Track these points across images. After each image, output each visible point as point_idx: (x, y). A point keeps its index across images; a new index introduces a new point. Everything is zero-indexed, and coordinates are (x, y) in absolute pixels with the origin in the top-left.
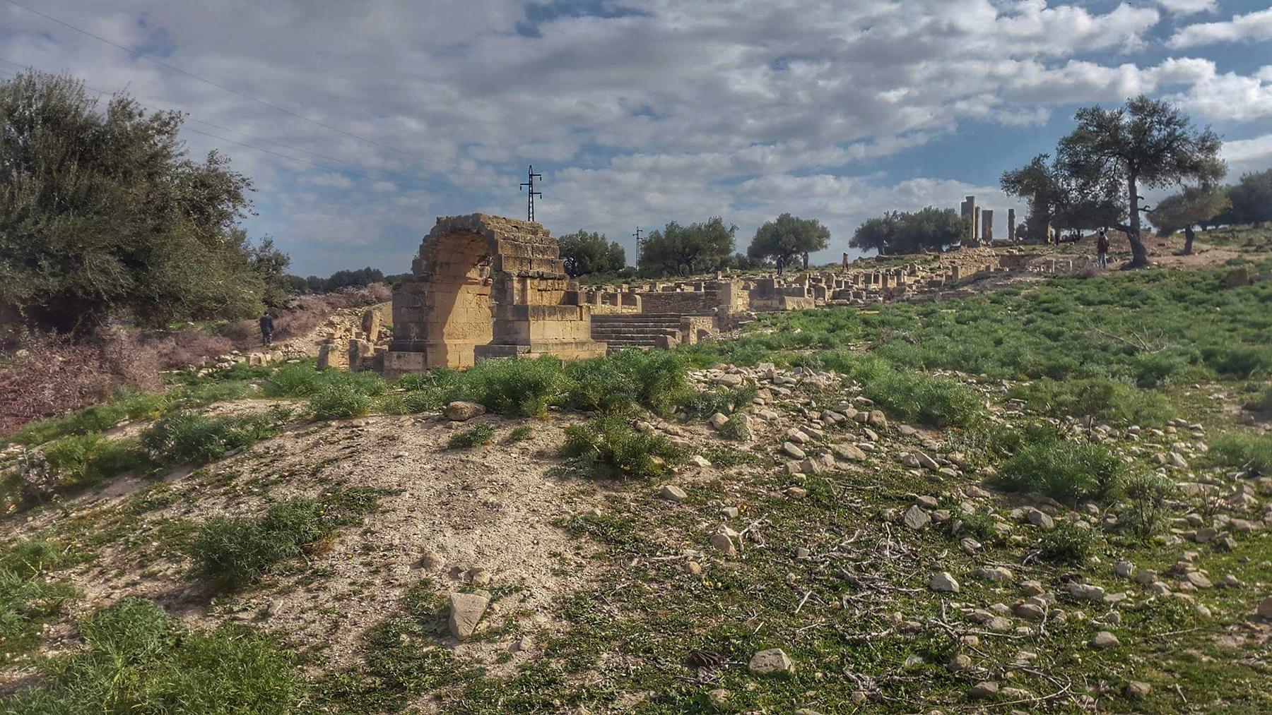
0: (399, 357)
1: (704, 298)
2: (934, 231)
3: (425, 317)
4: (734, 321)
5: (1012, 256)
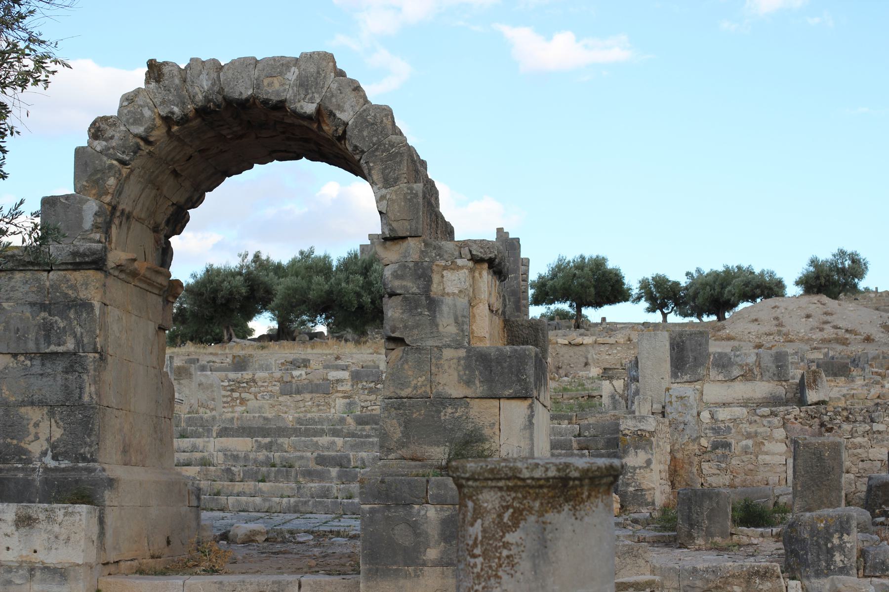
0: (24, 522)
1: (347, 387)
2: (358, 295)
3: (90, 390)
4: (716, 431)
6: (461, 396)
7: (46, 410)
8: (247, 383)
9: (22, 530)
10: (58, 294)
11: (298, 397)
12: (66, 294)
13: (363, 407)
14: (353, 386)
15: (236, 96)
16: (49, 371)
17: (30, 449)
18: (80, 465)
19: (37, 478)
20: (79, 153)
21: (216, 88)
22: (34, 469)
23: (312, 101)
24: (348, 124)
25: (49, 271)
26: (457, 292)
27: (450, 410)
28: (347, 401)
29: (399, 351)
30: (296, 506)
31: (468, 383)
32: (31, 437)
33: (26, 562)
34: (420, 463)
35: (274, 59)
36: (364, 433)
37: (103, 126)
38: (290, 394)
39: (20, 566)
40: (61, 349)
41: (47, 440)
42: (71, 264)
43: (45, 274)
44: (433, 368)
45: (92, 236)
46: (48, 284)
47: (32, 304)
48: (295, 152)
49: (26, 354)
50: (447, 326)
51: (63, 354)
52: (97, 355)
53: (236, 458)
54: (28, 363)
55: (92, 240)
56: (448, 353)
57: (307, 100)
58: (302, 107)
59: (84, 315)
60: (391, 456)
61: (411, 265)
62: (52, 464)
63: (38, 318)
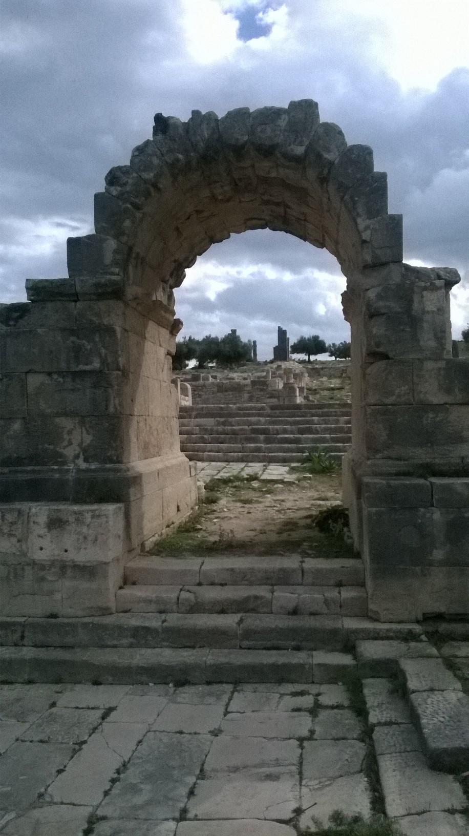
0: (56, 523)
1: (249, 388)
2: (229, 352)
3: (114, 402)
5: (313, 369)
6: (442, 402)
7: (77, 420)
8: (202, 387)
9: (54, 532)
10: (84, 321)
11: (226, 393)
12: (91, 320)
13: (257, 398)
14: (252, 387)
15: (233, 142)
16: (79, 386)
17: (65, 453)
18: (108, 466)
19: (71, 476)
20: (98, 197)
21: (216, 136)
22: (68, 471)
23: (301, 144)
24: (334, 163)
25: (76, 301)
26: (435, 309)
27: (431, 415)
28: (249, 395)
29: (384, 362)
30: (242, 458)
31: (448, 391)
32: (65, 443)
33: (57, 560)
34: (406, 462)
35: (266, 108)
36: (276, 415)
37: (119, 174)
38: (221, 392)
39: (53, 563)
40: (88, 368)
41: (79, 445)
42: (94, 294)
43: (73, 304)
44: (415, 378)
45: (113, 269)
46: (75, 312)
47: (63, 330)
48: (264, 219)
49: (60, 373)
50: (427, 341)
51: (91, 372)
52: (120, 373)
53: (206, 430)
54: (61, 380)
55: (113, 274)
56: (429, 365)
57: (296, 143)
58: (292, 150)
59: (107, 338)
60: (378, 456)
61: (393, 287)
62: (83, 465)
63: (68, 342)
